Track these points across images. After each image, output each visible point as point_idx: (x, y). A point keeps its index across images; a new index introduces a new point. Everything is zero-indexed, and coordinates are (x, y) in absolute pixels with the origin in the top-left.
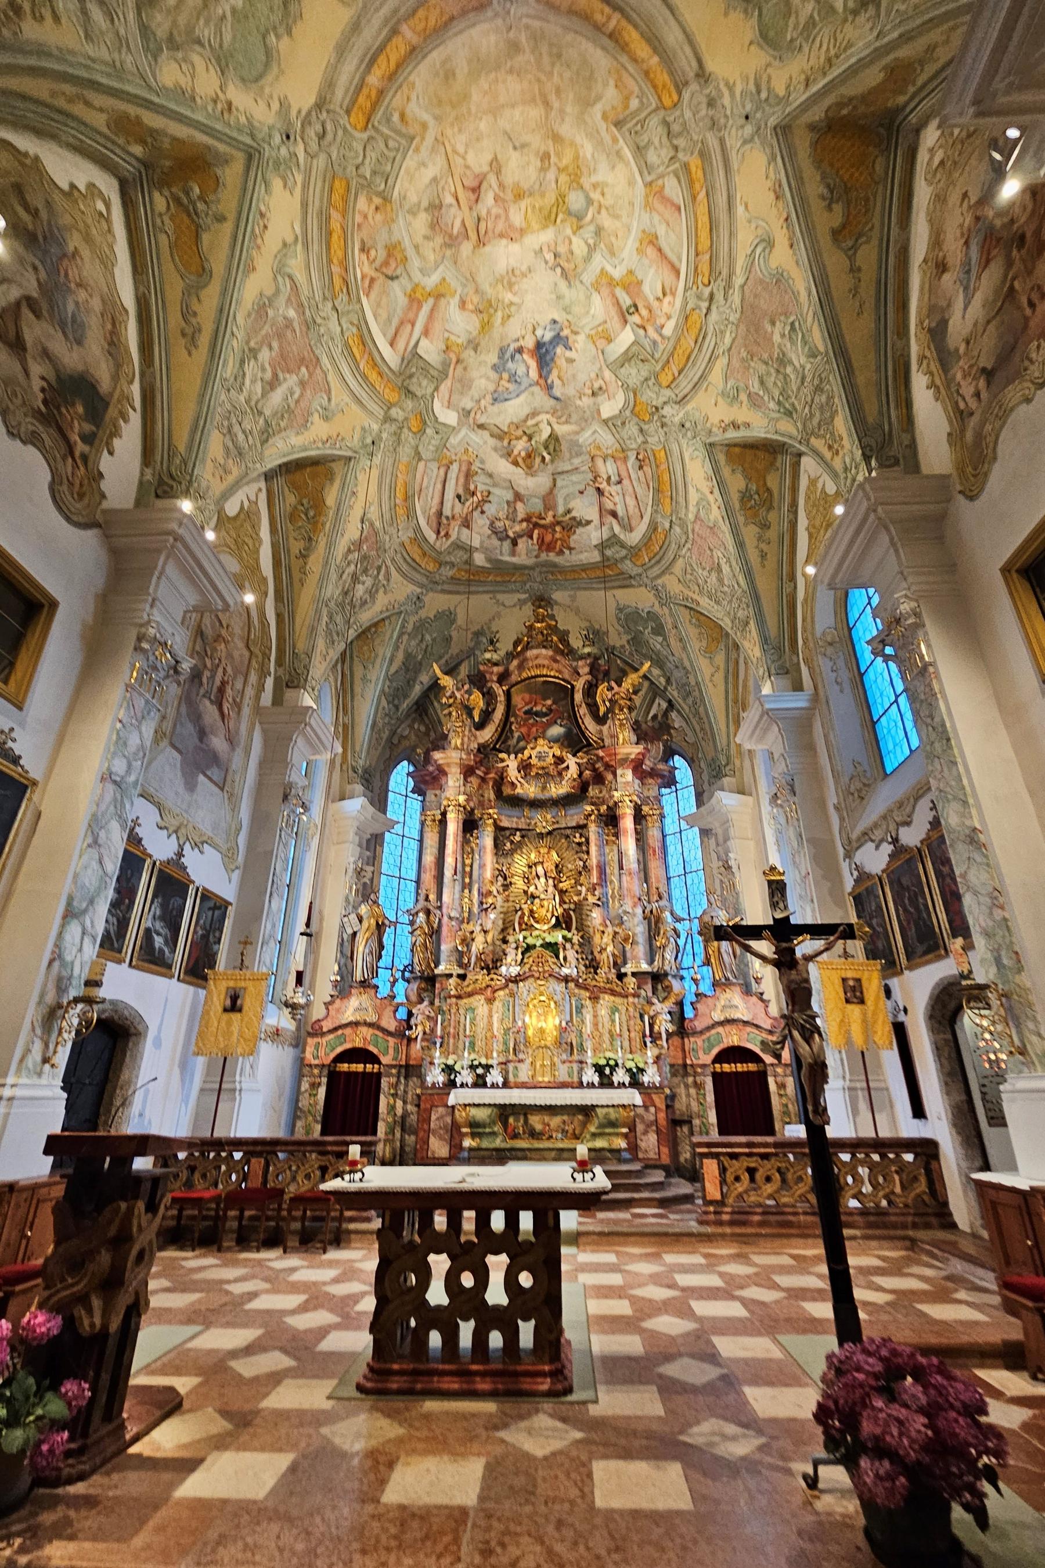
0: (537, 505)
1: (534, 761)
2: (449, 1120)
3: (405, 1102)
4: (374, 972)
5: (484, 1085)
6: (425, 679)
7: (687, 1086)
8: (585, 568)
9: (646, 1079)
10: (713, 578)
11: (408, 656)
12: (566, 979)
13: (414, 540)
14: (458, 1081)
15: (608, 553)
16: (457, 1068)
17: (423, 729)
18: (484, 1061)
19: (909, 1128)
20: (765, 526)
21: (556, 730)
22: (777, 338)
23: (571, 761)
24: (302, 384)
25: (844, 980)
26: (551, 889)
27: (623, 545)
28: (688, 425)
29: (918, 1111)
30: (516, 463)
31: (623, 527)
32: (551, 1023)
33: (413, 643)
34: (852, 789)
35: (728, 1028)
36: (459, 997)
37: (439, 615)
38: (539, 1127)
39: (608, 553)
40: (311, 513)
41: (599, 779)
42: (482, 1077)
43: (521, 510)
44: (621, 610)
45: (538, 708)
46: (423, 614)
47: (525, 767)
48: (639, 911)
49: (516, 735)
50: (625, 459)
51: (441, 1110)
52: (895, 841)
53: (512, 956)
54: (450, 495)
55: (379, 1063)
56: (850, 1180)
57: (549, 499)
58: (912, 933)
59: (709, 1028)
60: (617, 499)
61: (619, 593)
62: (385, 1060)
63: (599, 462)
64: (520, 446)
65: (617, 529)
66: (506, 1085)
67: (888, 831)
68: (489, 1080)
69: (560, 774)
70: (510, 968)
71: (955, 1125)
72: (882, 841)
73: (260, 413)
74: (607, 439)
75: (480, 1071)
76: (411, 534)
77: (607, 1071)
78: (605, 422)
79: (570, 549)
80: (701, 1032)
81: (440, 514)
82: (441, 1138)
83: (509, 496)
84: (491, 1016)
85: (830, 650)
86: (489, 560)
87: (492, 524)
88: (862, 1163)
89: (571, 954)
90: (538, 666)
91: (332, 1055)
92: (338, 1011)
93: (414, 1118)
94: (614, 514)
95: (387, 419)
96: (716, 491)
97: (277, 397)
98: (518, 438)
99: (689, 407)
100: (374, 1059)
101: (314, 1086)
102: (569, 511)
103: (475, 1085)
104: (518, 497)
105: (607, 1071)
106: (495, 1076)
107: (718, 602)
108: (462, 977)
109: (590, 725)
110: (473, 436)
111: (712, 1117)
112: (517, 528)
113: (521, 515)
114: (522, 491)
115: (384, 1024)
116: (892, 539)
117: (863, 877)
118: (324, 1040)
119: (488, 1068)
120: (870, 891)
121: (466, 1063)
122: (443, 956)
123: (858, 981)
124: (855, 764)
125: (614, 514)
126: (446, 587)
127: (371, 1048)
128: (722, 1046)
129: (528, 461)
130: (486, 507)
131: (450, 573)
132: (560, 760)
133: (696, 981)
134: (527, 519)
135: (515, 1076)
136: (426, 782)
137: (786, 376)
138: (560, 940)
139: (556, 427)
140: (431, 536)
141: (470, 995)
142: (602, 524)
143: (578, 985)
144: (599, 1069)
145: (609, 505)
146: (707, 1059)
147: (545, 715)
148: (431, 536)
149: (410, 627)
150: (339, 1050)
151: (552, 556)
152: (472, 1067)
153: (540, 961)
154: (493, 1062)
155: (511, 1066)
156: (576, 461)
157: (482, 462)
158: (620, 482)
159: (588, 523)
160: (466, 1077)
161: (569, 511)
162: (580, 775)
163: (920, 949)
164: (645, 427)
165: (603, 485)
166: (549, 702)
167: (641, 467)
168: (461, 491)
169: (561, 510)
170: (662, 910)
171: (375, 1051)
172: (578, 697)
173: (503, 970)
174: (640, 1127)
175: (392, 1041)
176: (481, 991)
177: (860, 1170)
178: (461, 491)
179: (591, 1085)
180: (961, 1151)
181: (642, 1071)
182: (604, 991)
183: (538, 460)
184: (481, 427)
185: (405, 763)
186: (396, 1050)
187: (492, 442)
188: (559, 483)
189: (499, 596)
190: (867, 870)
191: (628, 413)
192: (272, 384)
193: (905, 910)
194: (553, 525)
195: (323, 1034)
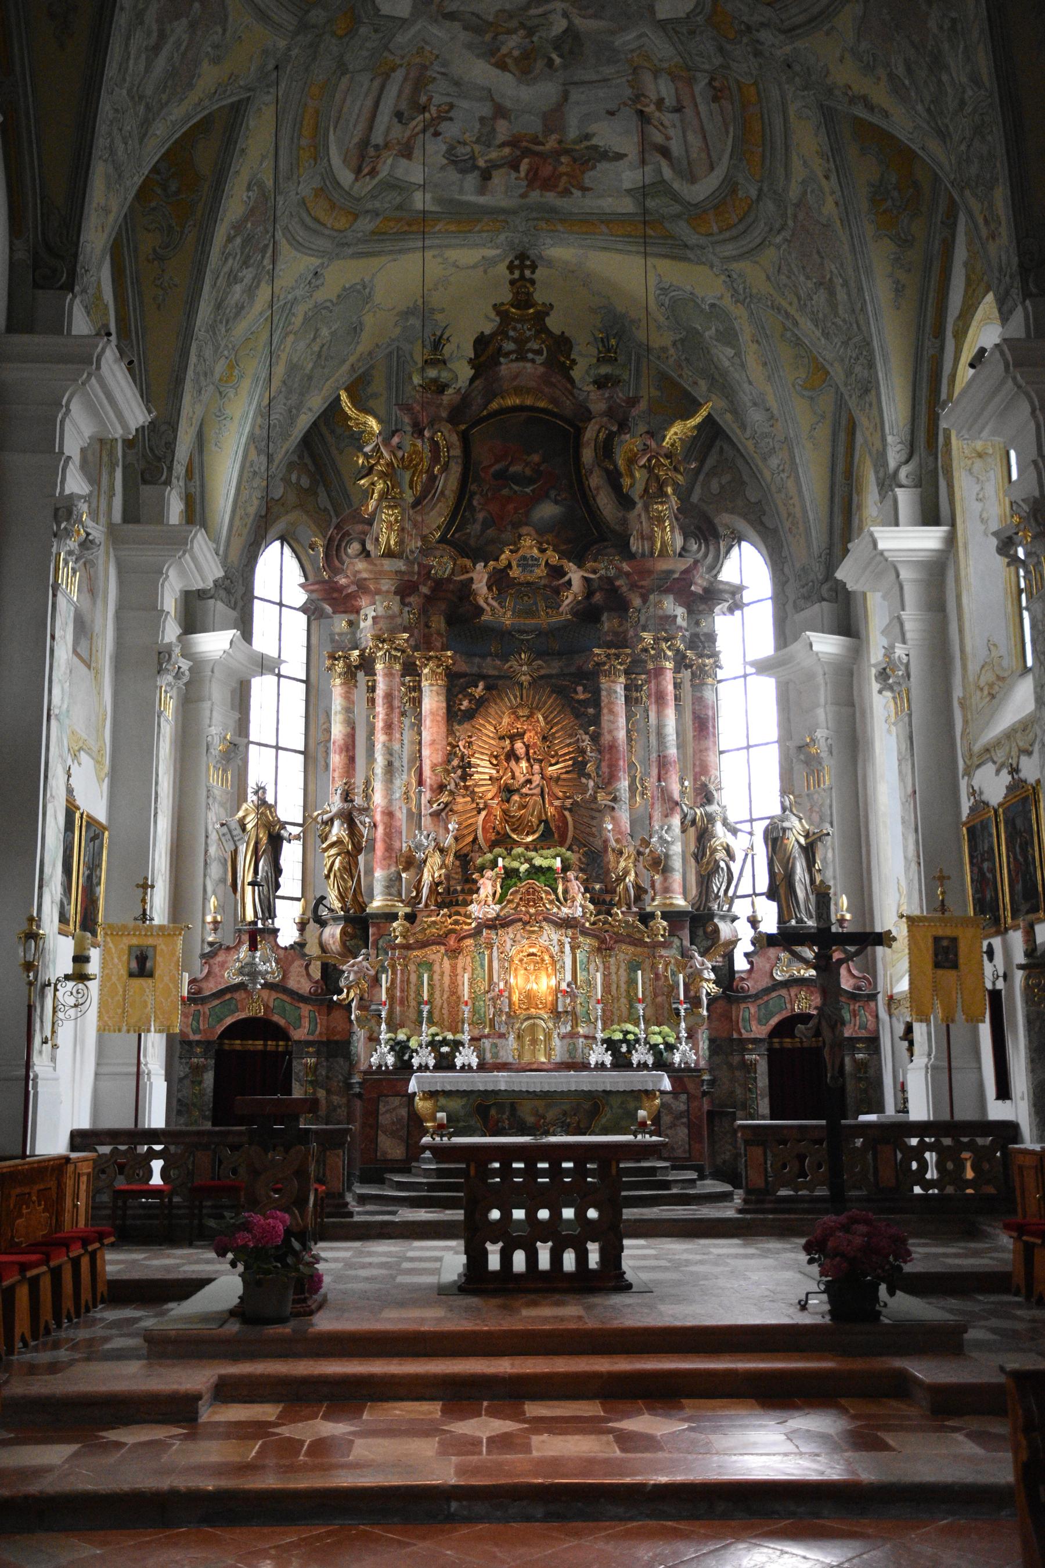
0: (533, 125)
1: (515, 573)
2: (404, 1112)
3: (329, 1092)
4: (269, 911)
5: (452, 1067)
6: (316, 403)
7: (731, 1067)
8: (610, 220)
9: (677, 1058)
10: (820, 298)
11: (293, 368)
12: (567, 923)
13: (320, 192)
14: (416, 1062)
15: (651, 204)
16: (413, 1044)
17: (305, 482)
18: (450, 1036)
19: (997, 1111)
20: (904, 242)
21: (547, 510)
22: (932, 24)
23: (575, 576)
24: (193, 26)
25: (937, 940)
26: (537, 779)
27: (676, 197)
28: (797, 68)
29: (1004, 1092)
30: (502, 66)
31: (679, 173)
32: (543, 984)
33: (302, 345)
34: (982, 682)
35: (793, 991)
36: (407, 947)
37: (347, 294)
38: (530, 1120)
39: (651, 204)
40: (173, 187)
41: (620, 605)
42: (451, 1056)
43: (503, 129)
44: (664, 291)
45: (515, 468)
46: (320, 296)
47: (500, 581)
48: (676, 821)
49: (480, 516)
50: (691, 82)
51: (396, 1101)
52: (1014, 770)
53: (487, 886)
54: (384, 117)
55: (286, 1037)
56: (914, 1165)
57: (554, 119)
58: (1019, 887)
59: (767, 991)
60: (671, 132)
61: (664, 266)
62: (299, 1034)
63: (647, 78)
64: (512, 43)
65: (667, 173)
66: (482, 1067)
67: (1009, 756)
68: (459, 1061)
69: (557, 591)
70: (484, 904)
71: (1035, 1105)
72: (1002, 765)
73: (141, 98)
74: (662, 49)
75: (445, 1049)
76: (316, 183)
77: (624, 1049)
78: (663, 25)
79: (584, 189)
80: (757, 996)
81: (365, 143)
82: (393, 1134)
83: (486, 110)
84: (454, 974)
85: (978, 464)
86: (439, 201)
87: (451, 149)
88: (930, 1148)
89: (576, 888)
90: (518, 391)
91: (220, 1029)
92: (223, 965)
93: (342, 1112)
94: (665, 152)
95: (303, 27)
96: (833, 177)
97: (161, 64)
98: (510, 32)
99: (799, 44)
100: (279, 1033)
101: (197, 1071)
102: (587, 137)
103: (437, 1068)
104: (500, 112)
105: (624, 1049)
106: (466, 1057)
107: (826, 335)
108: (411, 918)
109: (605, 503)
110: (434, 30)
111: (764, 1106)
112: (494, 155)
113: (501, 138)
114: (508, 104)
115: (292, 984)
116: (1033, 412)
117: (980, 806)
118: (206, 1009)
119: (457, 1045)
120: (985, 826)
121: (425, 1038)
122: (378, 888)
123: (954, 940)
124: (991, 645)
125: (665, 152)
126: (362, 248)
127: (276, 1018)
128: (785, 1014)
129: (524, 65)
130: (444, 126)
131: (371, 227)
132: (557, 572)
133: (754, 922)
134: (513, 143)
135: (495, 1055)
136: (334, 603)
137: (940, 81)
138: (558, 863)
139: (577, 21)
140: (346, 177)
141: (423, 945)
142: (643, 162)
143: (584, 933)
144: (611, 1045)
145: (658, 138)
146: (759, 1031)
147: (531, 481)
148: (346, 177)
149: (298, 321)
150: (229, 1021)
151: (551, 198)
152: (434, 1045)
153: (531, 898)
154: (466, 1037)
155: (487, 1043)
156: (608, 71)
157: (445, 64)
158: (678, 109)
159: (619, 156)
160: (425, 1057)
161: (587, 137)
162: (589, 594)
163: (1024, 908)
164: (728, 47)
165: (651, 109)
166: (536, 458)
167: (716, 99)
168: (403, 106)
169: (572, 133)
170: (710, 818)
171: (282, 1022)
172: (588, 455)
173: (474, 909)
174: (666, 1119)
175: (305, 1009)
176: (440, 940)
177: (927, 1155)
178: (403, 106)
179: (601, 1066)
180: (1035, 1132)
181: (670, 1048)
182: (619, 939)
183: (540, 64)
184: (451, 16)
185: (277, 544)
186: (313, 1021)
187: (464, 36)
188: (575, 95)
189: (453, 254)
190: (985, 797)
191: (700, 19)
192: (156, 49)
193: (1015, 858)
194: (557, 154)
195: (204, 1000)
